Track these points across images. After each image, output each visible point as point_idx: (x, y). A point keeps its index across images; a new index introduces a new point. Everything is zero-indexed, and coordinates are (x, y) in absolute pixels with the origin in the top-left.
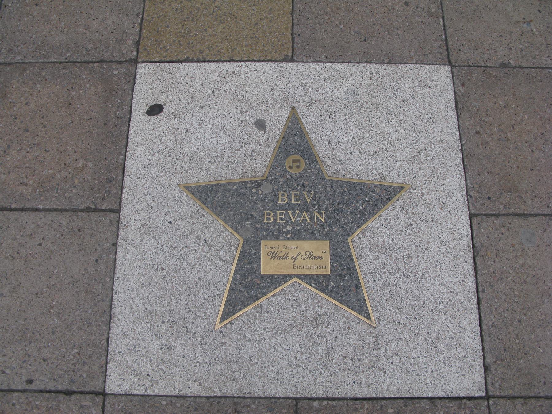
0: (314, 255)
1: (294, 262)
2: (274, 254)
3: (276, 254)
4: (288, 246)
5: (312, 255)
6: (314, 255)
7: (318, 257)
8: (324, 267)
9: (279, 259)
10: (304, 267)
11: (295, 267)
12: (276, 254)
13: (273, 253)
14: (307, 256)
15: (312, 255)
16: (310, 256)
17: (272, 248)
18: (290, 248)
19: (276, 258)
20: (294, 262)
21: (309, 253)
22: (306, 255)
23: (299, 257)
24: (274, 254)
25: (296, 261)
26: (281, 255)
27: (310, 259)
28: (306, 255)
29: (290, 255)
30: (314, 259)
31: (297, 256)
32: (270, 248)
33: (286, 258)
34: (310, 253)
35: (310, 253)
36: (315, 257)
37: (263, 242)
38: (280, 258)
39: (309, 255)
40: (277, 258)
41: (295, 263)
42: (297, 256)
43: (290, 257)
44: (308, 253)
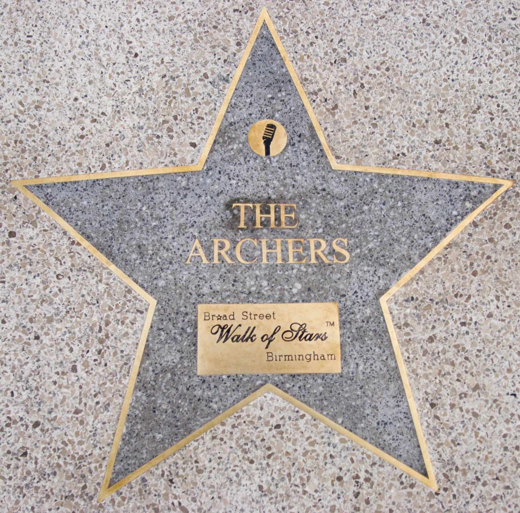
0: (309, 331)
1: (267, 347)
2: (225, 331)
3: (228, 331)
7: (318, 336)
9: (237, 341)
10: (288, 357)
13: (223, 329)
14: (295, 333)
17: (219, 318)
18: (257, 317)
19: (230, 340)
20: (267, 347)
21: (299, 326)
22: (292, 330)
24: (225, 331)
25: (271, 343)
26: (241, 332)
27: (300, 340)
29: (258, 334)
30: (310, 339)
31: (274, 333)
32: (215, 318)
33: (250, 338)
34: (301, 326)
36: (311, 335)
37: (201, 308)
38: (238, 339)
40: (232, 339)
41: (268, 350)
42: (274, 333)
44: (296, 327)
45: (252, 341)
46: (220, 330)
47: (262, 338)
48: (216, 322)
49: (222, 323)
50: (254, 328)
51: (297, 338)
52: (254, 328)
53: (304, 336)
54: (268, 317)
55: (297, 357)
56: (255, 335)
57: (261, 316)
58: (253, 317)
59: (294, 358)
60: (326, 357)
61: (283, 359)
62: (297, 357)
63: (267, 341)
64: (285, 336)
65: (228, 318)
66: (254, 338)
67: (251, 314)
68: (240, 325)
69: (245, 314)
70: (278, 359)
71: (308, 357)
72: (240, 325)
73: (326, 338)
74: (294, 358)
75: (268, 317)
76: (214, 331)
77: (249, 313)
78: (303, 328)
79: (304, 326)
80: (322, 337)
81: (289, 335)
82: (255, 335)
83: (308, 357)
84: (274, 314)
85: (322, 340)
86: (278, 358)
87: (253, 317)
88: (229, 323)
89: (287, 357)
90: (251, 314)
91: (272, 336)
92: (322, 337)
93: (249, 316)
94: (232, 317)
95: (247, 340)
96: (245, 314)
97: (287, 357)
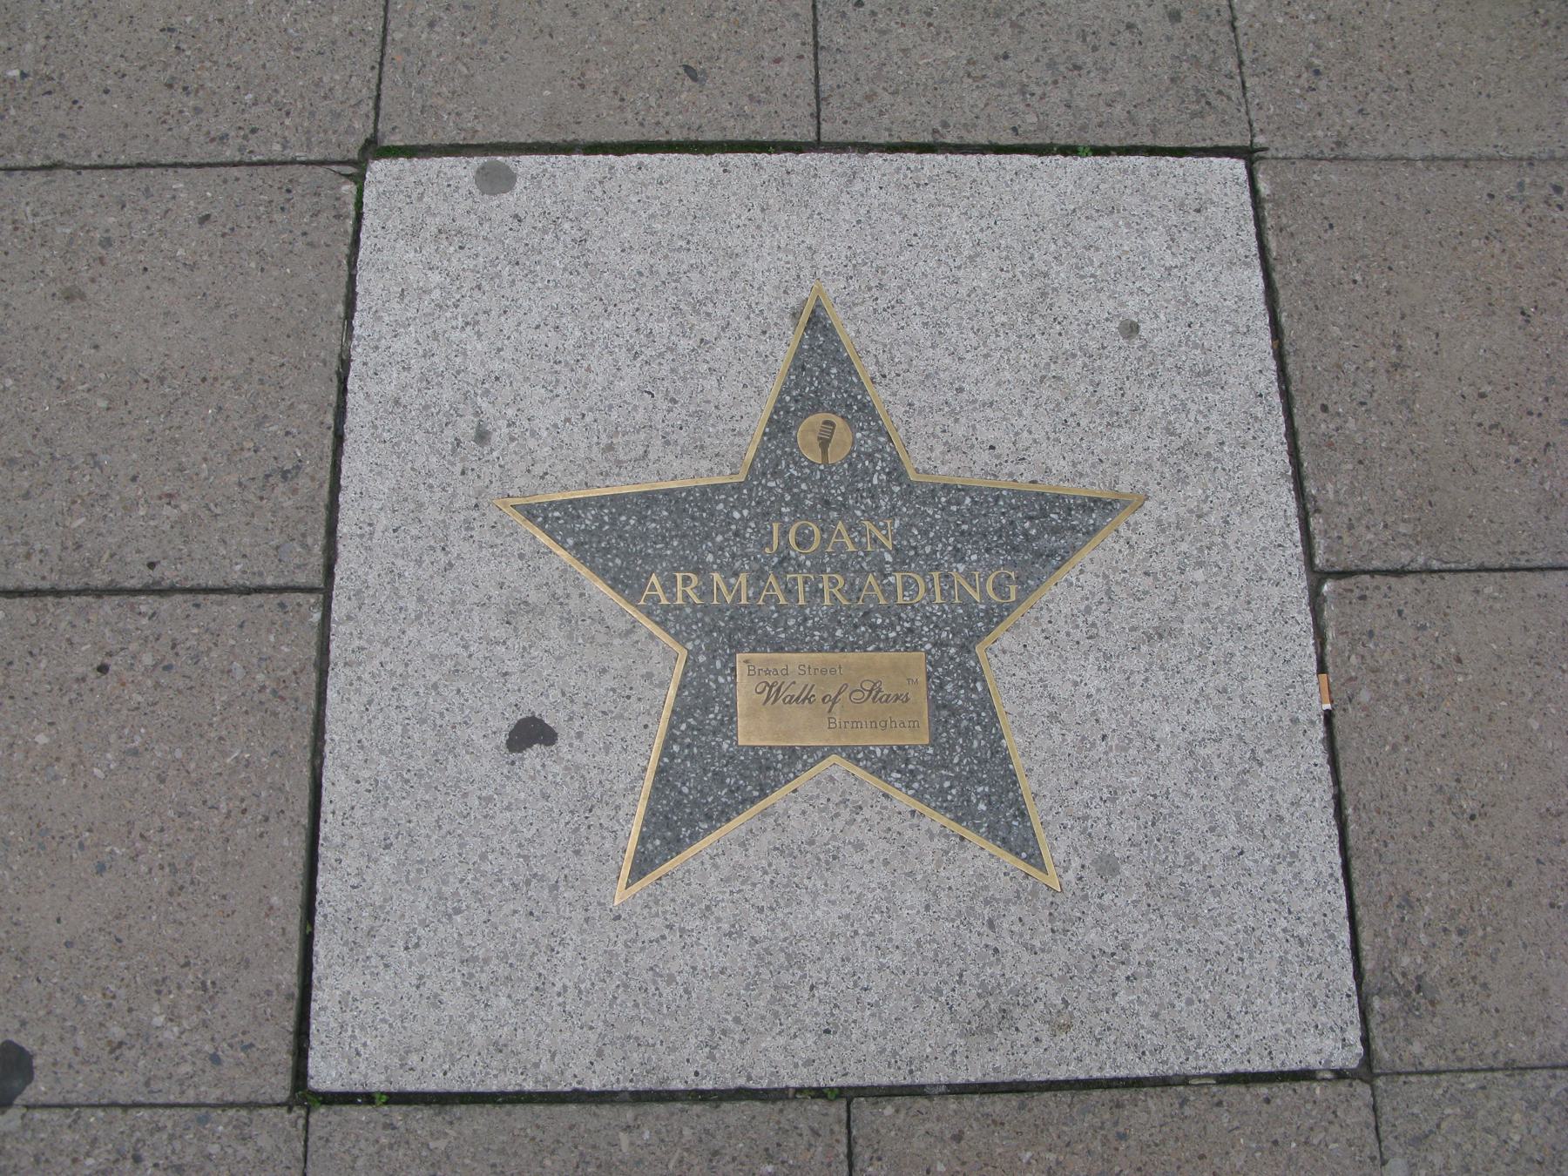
3: (778, 690)
5: (880, 691)
8: (914, 726)
9: (790, 702)
12: (778, 690)
14: (866, 693)
15: (880, 691)
19: (780, 701)
23: (845, 694)
31: (839, 693)
39: (871, 691)
42: (839, 693)
43: (819, 697)
44: (868, 686)
47: (823, 699)
58: (812, 671)
60: (907, 724)
87: (812, 671)
95: (803, 701)
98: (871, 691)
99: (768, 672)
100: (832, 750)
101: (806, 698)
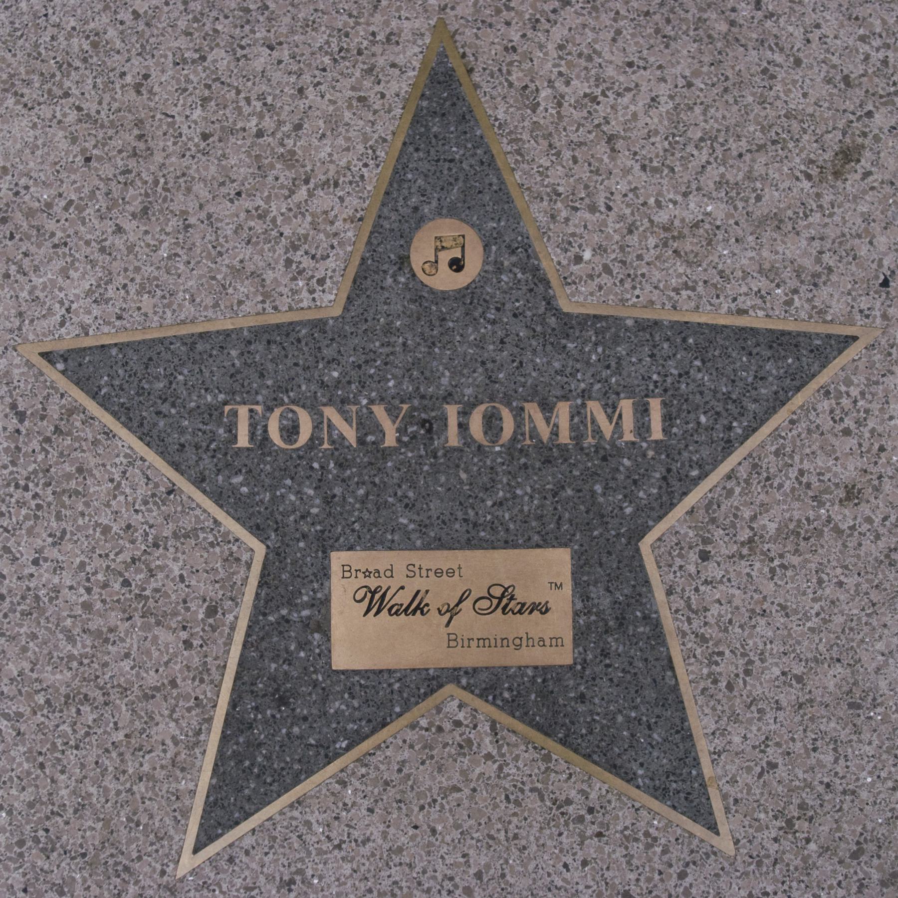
2: (377, 596)
4: (424, 568)
5: (512, 598)
6: (521, 595)
7: (534, 607)
9: (396, 613)
11: (452, 644)
13: (373, 593)
14: (495, 602)
15: (512, 598)
16: (505, 601)
17: (367, 574)
19: (385, 611)
23: (467, 604)
24: (377, 596)
26: (403, 598)
27: (504, 613)
28: (491, 597)
29: (434, 601)
31: (460, 601)
32: (360, 575)
35: (506, 589)
36: (523, 605)
39: (503, 596)
40: (390, 610)
41: (450, 629)
42: (460, 601)
43: (433, 608)
44: (497, 592)
45: (422, 613)
46: (369, 595)
48: (362, 581)
49: (373, 583)
50: (427, 592)
51: (499, 610)
52: (427, 592)
53: (510, 606)
54: (450, 573)
55: (499, 641)
56: (427, 605)
57: (438, 573)
58: (424, 573)
59: (493, 644)
60: (548, 643)
61: (474, 644)
62: (499, 641)
63: (448, 615)
64: (477, 604)
65: (382, 574)
66: (425, 610)
67: (420, 569)
68: (402, 588)
69: (411, 568)
70: (466, 643)
71: (517, 641)
72: (402, 588)
73: (547, 610)
74: (493, 644)
75: (450, 573)
76: (358, 597)
77: (417, 566)
78: (507, 595)
79: (510, 590)
80: (543, 609)
81: (485, 604)
82: (427, 605)
83: (517, 641)
84: (460, 568)
85: (542, 613)
86: (466, 643)
87: (424, 573)
88: (384, 583)
89: (481, 642)
90: (420, 569)
91: (457, 605)
92: (543, 609)
93: (417, 572)
94: (388, 574)
95: (414, 612)
96: (411, 568)
97: (481, 642)
98: (500, 599)
99: (367, 574)
100: (454, 675)
101: (417, 608)
